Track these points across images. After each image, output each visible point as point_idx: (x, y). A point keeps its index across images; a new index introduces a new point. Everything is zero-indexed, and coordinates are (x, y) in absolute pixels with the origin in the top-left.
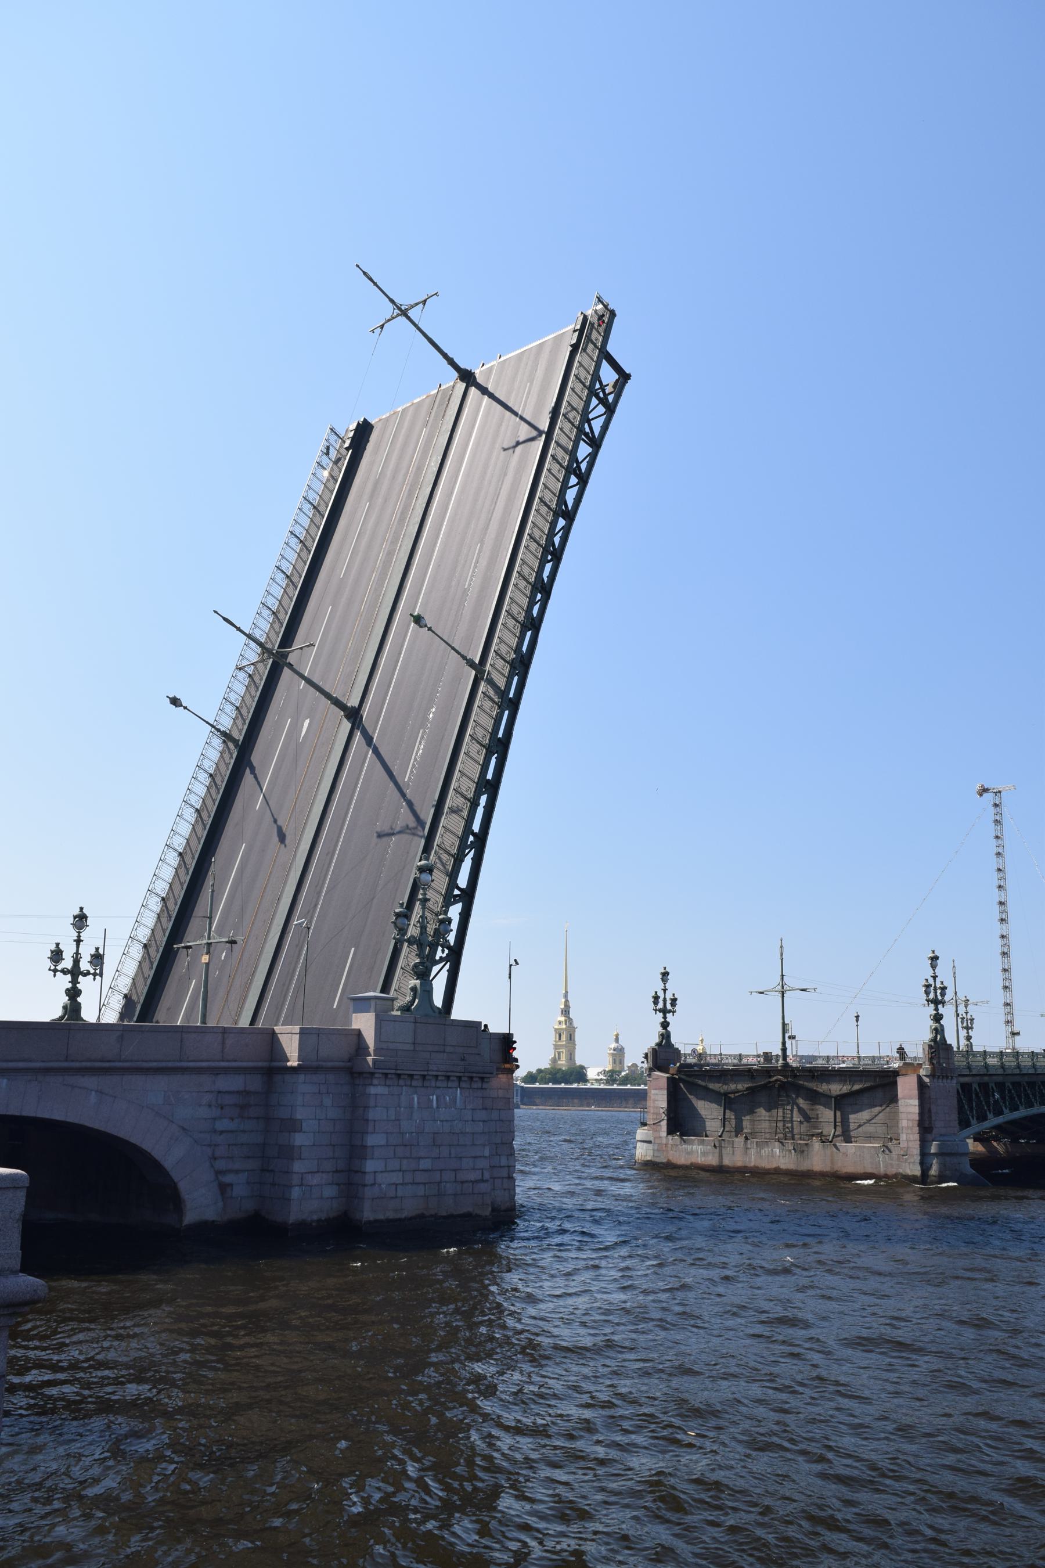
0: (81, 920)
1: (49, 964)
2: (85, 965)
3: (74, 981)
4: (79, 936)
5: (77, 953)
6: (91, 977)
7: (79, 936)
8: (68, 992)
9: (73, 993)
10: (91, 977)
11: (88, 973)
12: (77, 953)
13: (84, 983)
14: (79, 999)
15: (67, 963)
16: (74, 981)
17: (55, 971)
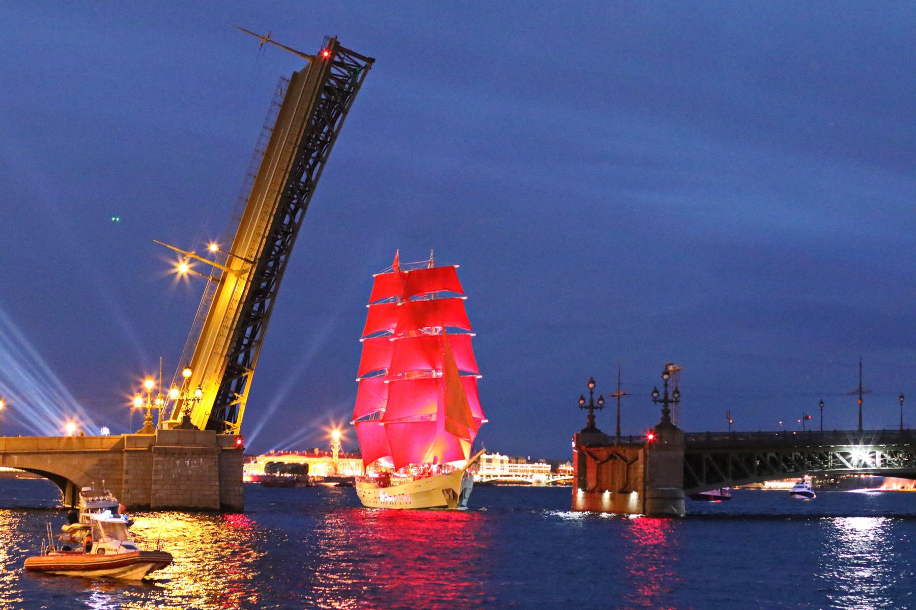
2: (595, 404)
3: (592, 412)
9: (592, 417)
11: (597, 408)
16: (592, 412)
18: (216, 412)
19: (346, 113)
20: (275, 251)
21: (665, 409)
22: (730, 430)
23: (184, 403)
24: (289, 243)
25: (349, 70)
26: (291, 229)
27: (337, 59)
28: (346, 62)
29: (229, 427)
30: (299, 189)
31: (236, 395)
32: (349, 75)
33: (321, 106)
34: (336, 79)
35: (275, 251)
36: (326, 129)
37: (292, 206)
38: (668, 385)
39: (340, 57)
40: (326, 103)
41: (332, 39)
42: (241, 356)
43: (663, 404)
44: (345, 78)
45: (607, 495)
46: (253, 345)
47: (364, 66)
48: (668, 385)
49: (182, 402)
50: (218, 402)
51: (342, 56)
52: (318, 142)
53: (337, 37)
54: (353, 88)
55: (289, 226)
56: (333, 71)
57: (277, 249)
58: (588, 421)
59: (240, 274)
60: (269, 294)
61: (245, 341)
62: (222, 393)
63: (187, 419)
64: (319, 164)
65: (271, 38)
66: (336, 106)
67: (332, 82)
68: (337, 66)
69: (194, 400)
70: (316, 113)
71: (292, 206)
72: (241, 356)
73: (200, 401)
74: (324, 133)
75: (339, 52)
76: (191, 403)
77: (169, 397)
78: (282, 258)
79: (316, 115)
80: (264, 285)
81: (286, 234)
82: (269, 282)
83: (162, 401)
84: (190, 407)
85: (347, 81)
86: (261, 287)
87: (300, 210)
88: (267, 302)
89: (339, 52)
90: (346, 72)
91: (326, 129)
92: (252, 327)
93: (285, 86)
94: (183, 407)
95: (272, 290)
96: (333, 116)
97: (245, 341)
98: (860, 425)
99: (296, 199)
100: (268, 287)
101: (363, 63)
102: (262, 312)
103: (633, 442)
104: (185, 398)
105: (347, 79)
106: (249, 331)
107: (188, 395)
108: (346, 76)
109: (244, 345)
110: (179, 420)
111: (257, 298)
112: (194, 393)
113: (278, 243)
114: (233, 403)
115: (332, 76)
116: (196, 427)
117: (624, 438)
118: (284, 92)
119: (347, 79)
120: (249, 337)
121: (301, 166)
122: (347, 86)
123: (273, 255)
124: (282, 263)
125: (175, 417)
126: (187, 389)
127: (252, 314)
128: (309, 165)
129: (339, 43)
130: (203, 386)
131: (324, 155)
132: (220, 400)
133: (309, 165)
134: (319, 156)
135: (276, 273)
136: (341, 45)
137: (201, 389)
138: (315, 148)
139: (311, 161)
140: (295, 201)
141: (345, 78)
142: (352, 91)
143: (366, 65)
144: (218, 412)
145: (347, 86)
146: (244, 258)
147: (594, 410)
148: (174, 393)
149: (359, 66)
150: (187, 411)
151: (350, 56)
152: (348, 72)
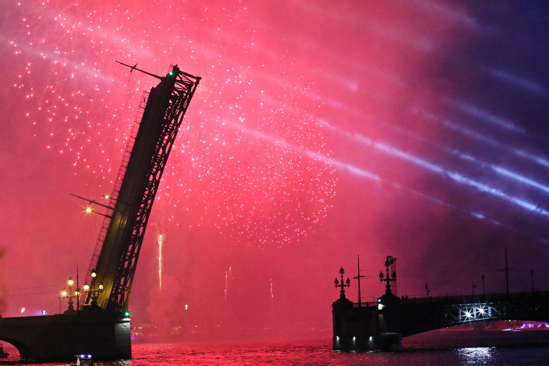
0: (342, 271)
1: (379, 278)
2: (345, 283)
3: (342, 288)
4: (342, 275)
5: (388, 274)
6: (347, 287)
7: (342, 275)
8: (341, 292)
9: (343, 292)
10: (347, 287)
11: (346, 286)
12: (388, 274)
13: (345, 289)
14: (345, 293)
15: (340, 283)
16: (342, 288)
17: (382, 280)
18: (112, 298)
19: (185, 111)
20: (145, 197)
21: (387, 285)
22: (428, 296)
23: (92, 293)
24: (153, 193)
25: (186, 85)
26: (154, 184)
27: (178, 78)
28: (184, 80)
29: (121, 307)
30: (158, 159)
31: (124, 287)
32: (186, 88)
33: (170, 107)
34: (178, 91)
35: (145, 197)
36: (173, 121)
37: (154, 170)
38: (389, 270)
39: (180, 77)
40: (173, 105)
41: (174, 66)
42: (126, 263)
43: (386, 282)
44: (184, 90)
45: (354, 338)
46: (134, 256)
47: (194, 82)
48: (389, 270)
49: (91, 293)
50: (113, 292)
51: (181, 76)
52: (169, 130)
53: (177, 65)
54: (188, 96)
55: (152, 182)
56: (176, 86)
57: (146, 196)
58: (340, 294)
59: (123, 214)
60: (142, 224)
61: (129, 254)
62: (115, 286)
63: (94, 303)
64: (169, 143)
65: (137, 67)
66: (178, 107)
67: (176, 92)
68: (178, 83)
69: (98, 291)
70: (166, 112)
71: (154, 170)
72: (126, 263)
73: (102, 292)
74: (172, 124)
75: (179, 74)
76: (97, 293)
77: (83, 290)
78: (149, 202)
79: (166, 113)
80: (138, 218)
81: (152, 186)
82: (142, 217)
83: (79, 293)
84: (96, 295)
85: (185, 91)
86: (137, 220)
87: (159, 172)
88: (141, 229)
89: (179, 74)
90: (184, 86)
91: (173, 121)
92: (132, 245)
93: (147, 96)
94: (92, 296)
95: (144, 221)
96: (177, 114)
97: (129, 254)
98: (508, 290)
99: (156, 165)
100: (141, 220)
101: (195, 80)
102: (138, 235)
103: (369, 306)
104: (93, 290)
105: (185, 90)
106: (130, 247)
107: (95, 289)
108: (184, 89)
109: (128, 256)
110: (90, 304)
111: (135, 227)
112: (99, 287)
113: (146, 192)
114: (123, 292)
115: (175, 89)
116: (100, 308)
117: (363, 303)
118: (146, 100)
119: (185, 90)
120: (130, 251)
121: (158, 145)
122: (185, 95)
123: (143, 200)
124: (149, 205)
125: (87, 302)
126: (94, 284)
127: (132, 237)
128: (164, 144)
129: (179, 69)
130: (104, 282)
131: (172, 138)
132: (114, 290)
133: (164, 144)
134: (170, 138)
135: (146, 211)
136: (181, 70)
137: (102, 284)
138: (167, 133)
139: (165, 142)
140: (156, 167)
141: (184, 90)
142: (188, 97)
143: (196, 82)
144: (113, 298)
145: (185, 95)
146: (126, 202)
147: (344, 287)
148: (86, 288)
149: (192, 82)
150: (95, 299)
151: (186, 76)
152: (185, 86)
